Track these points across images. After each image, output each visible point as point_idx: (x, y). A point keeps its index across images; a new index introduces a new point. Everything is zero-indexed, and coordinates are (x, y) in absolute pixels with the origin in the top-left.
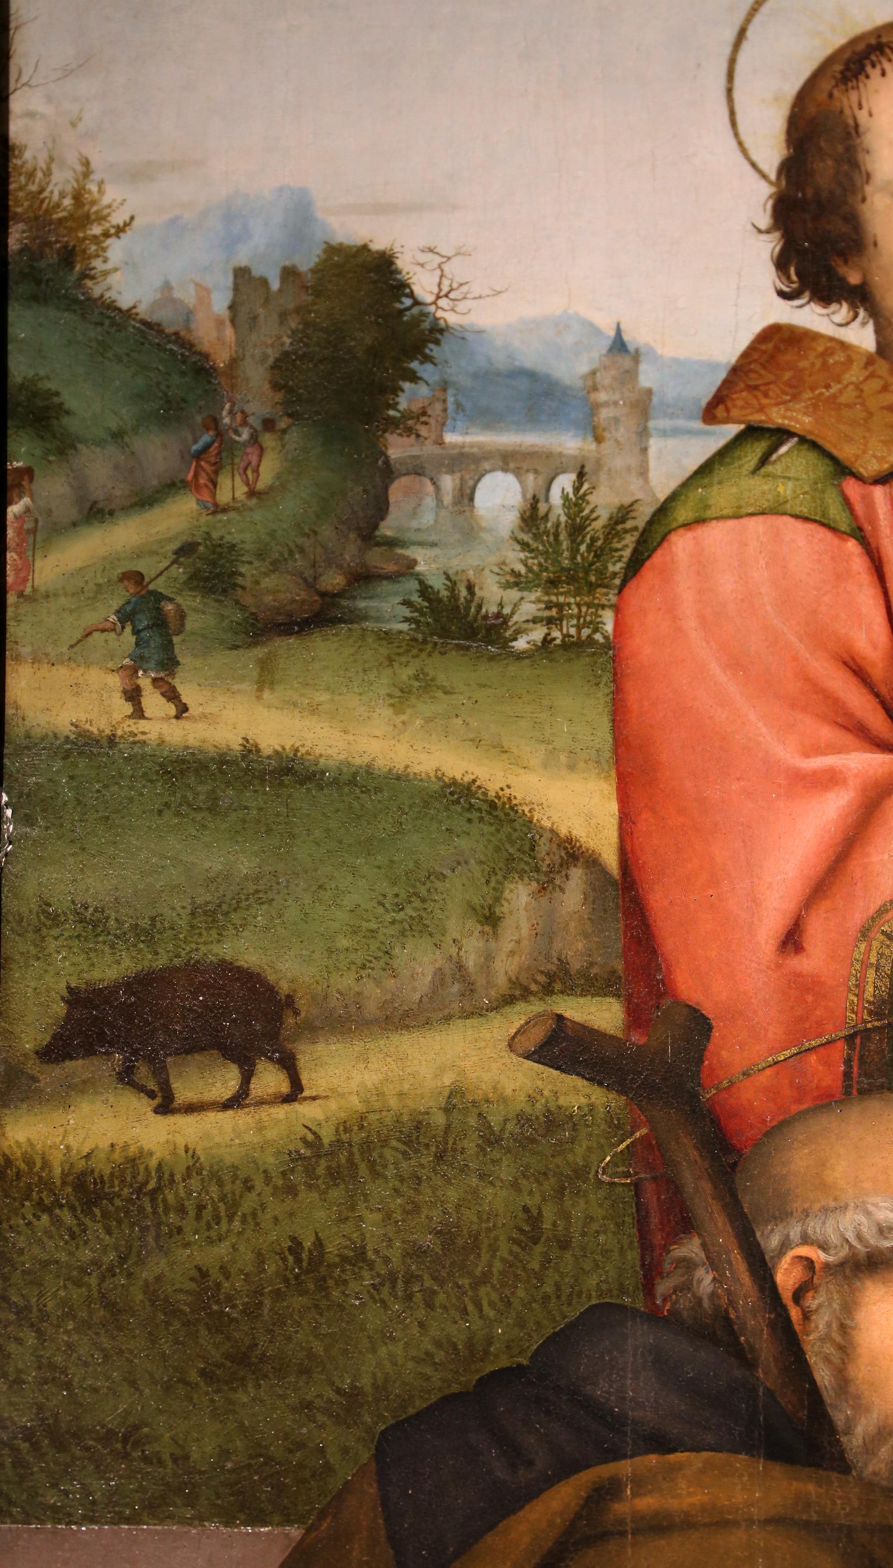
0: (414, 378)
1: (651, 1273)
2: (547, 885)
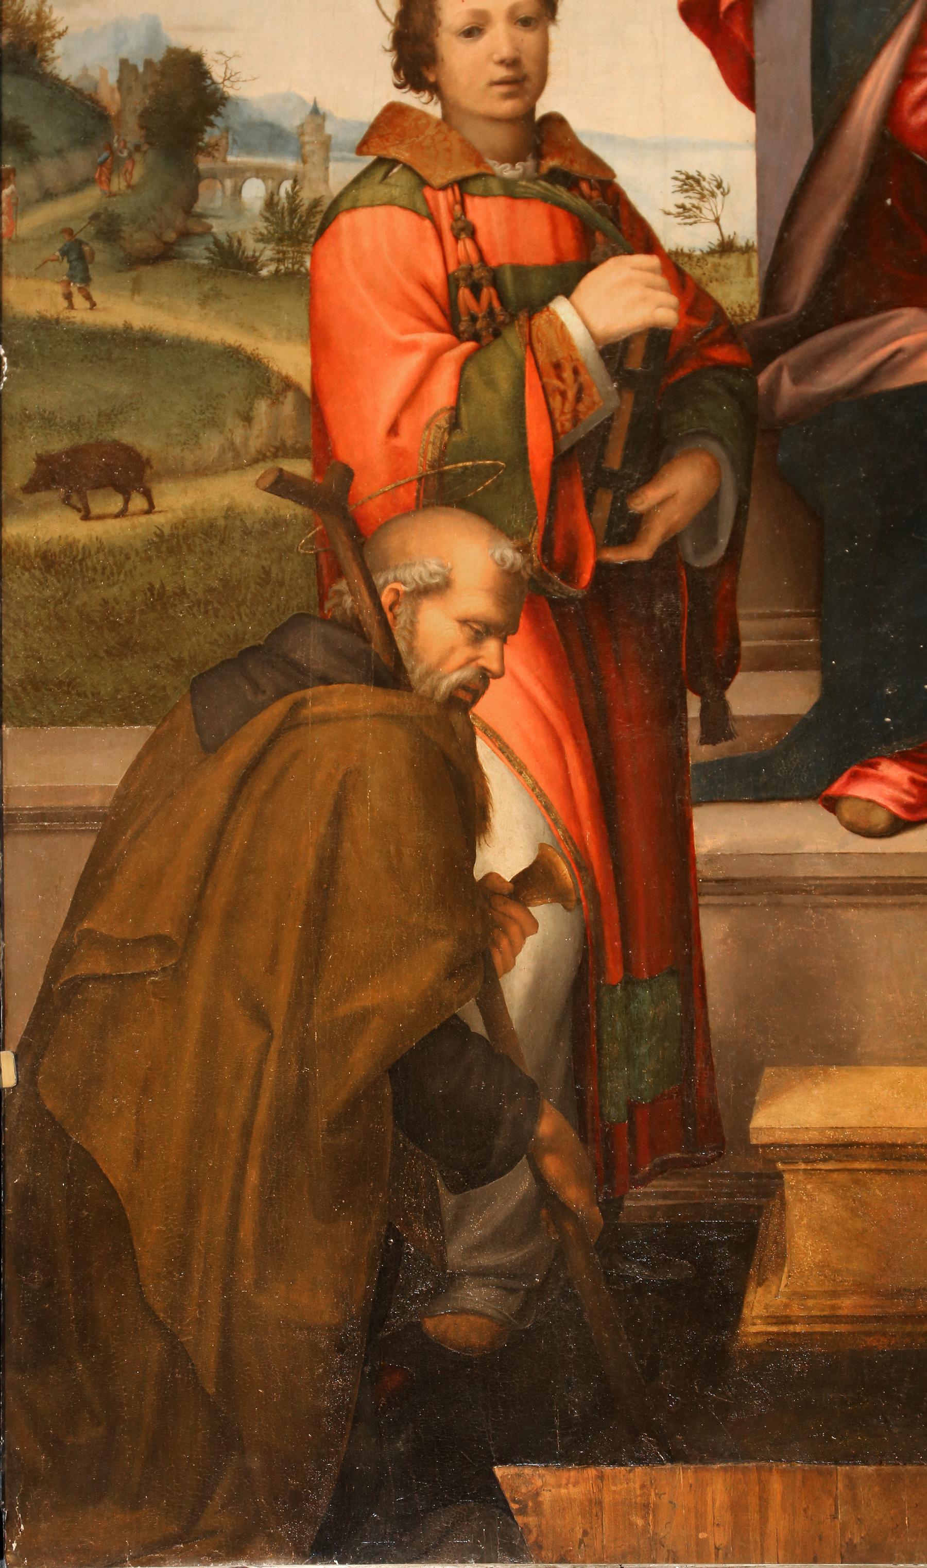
0: (212, 125)
1: (323, 598)
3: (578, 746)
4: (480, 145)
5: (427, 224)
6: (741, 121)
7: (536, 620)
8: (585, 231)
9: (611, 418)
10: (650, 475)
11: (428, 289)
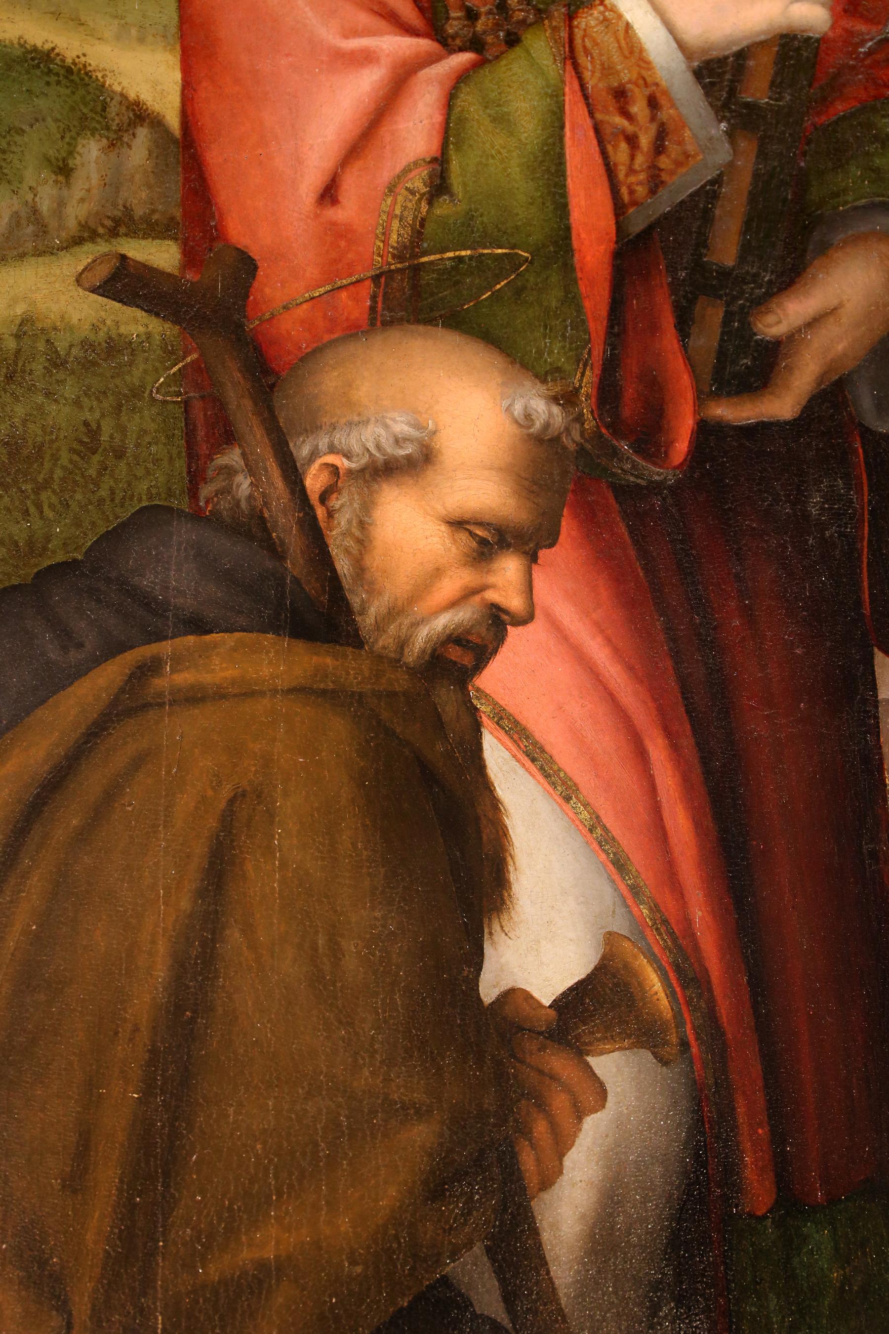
1: (196, 478)
2: (116, 142)
3: (674, 747)
7: (590, 518)
9: (717, 181)
10: (791, 276)
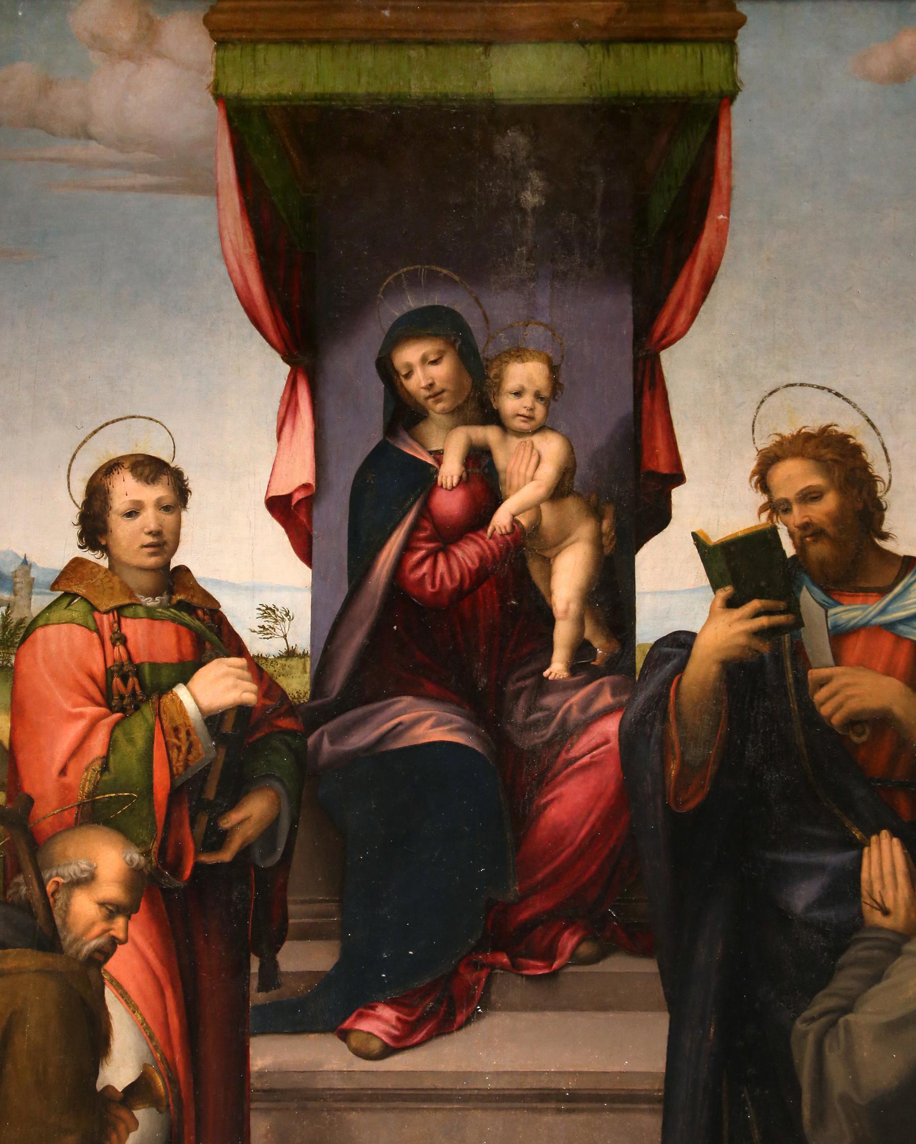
4: (132, 585)
5: (95, 635)
6: (303, 574)
7: (152, 903)
8: (199, 641)
9: (210, 765)
10: (234, 803)
11: (92, 678)
